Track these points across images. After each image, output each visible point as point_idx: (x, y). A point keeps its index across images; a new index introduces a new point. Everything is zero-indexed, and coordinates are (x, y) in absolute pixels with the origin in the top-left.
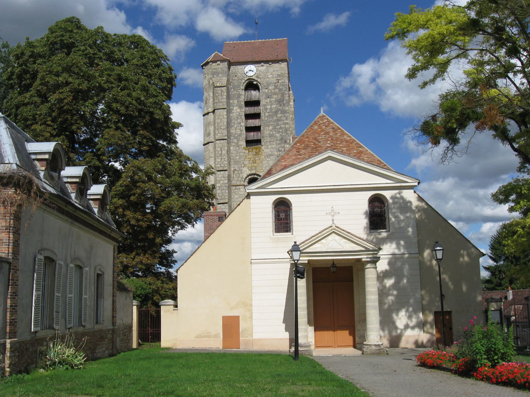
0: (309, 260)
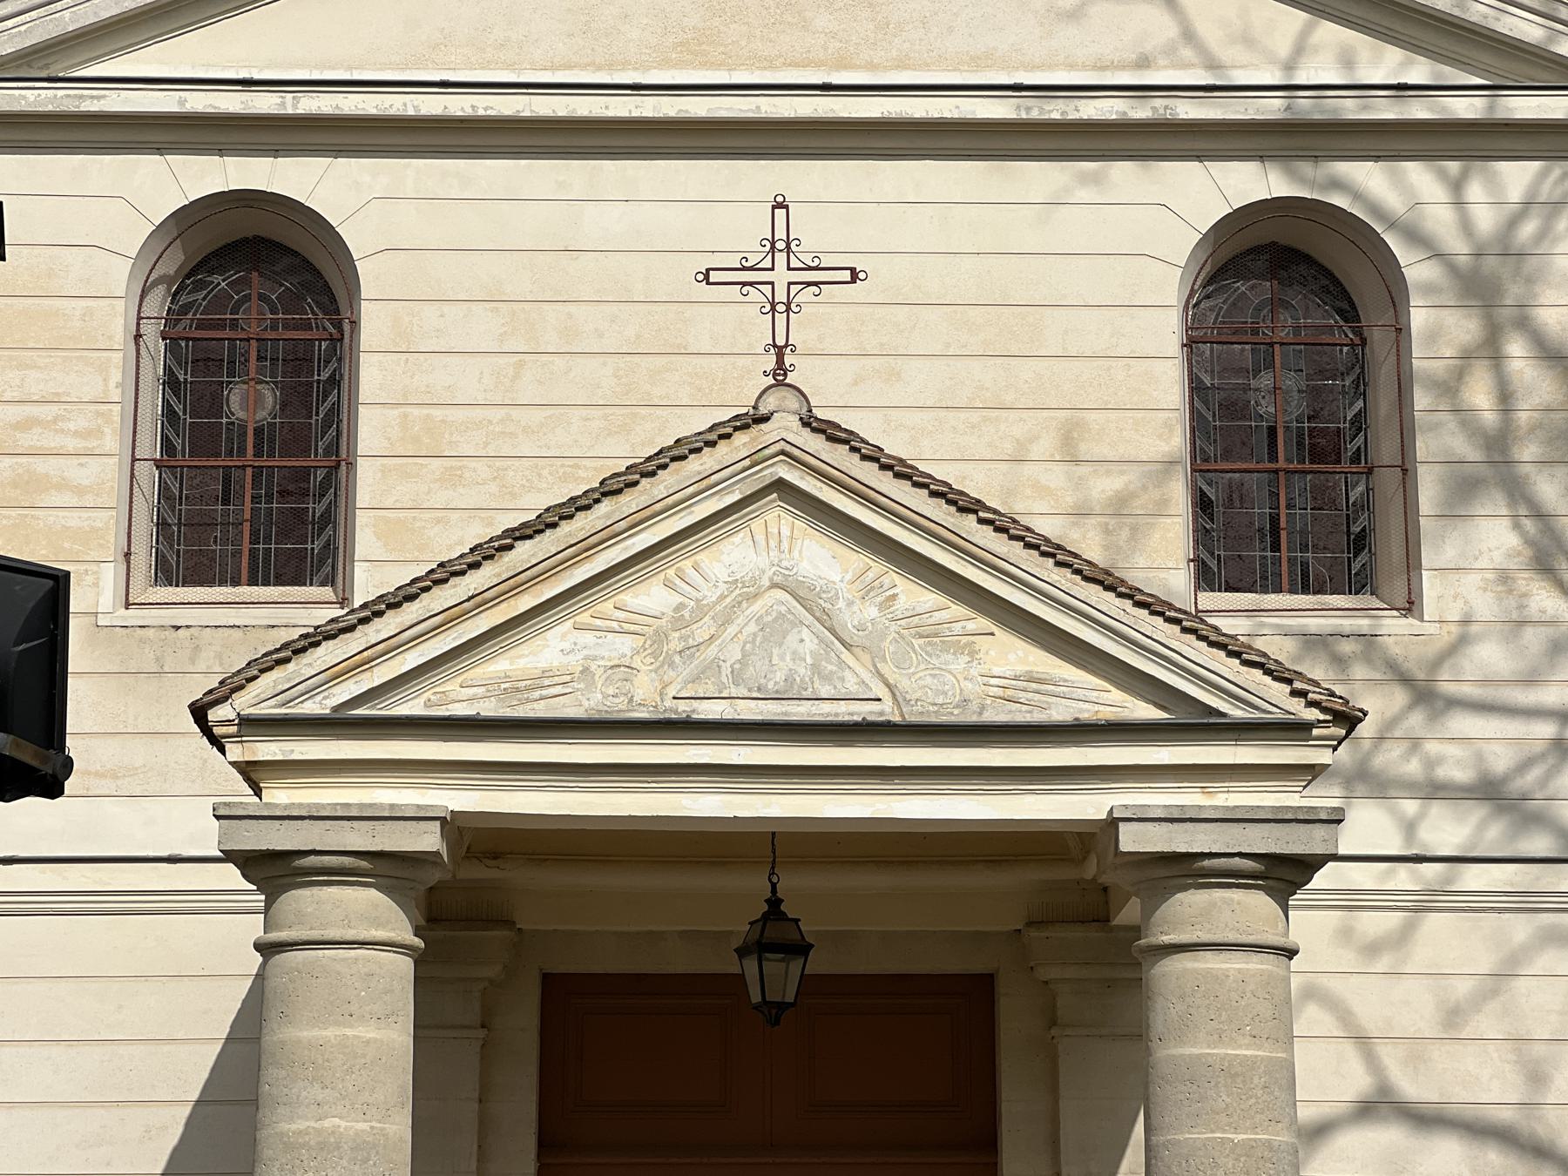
0: (454, 825)
